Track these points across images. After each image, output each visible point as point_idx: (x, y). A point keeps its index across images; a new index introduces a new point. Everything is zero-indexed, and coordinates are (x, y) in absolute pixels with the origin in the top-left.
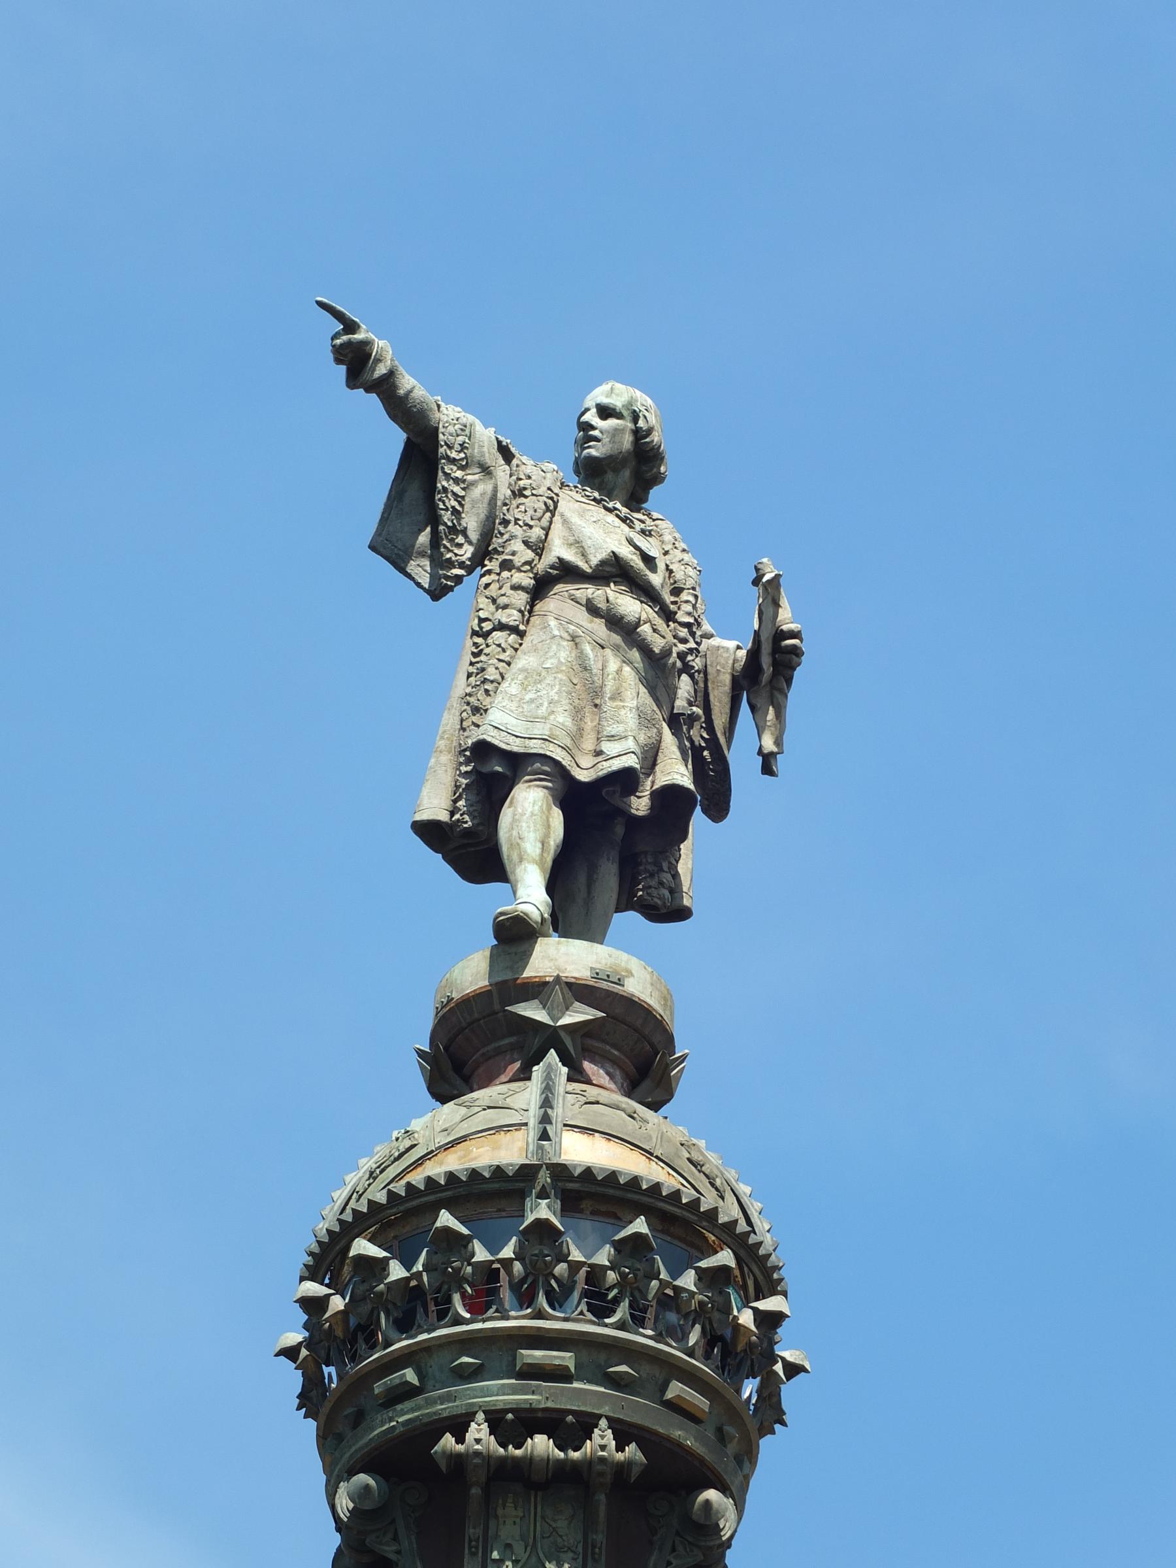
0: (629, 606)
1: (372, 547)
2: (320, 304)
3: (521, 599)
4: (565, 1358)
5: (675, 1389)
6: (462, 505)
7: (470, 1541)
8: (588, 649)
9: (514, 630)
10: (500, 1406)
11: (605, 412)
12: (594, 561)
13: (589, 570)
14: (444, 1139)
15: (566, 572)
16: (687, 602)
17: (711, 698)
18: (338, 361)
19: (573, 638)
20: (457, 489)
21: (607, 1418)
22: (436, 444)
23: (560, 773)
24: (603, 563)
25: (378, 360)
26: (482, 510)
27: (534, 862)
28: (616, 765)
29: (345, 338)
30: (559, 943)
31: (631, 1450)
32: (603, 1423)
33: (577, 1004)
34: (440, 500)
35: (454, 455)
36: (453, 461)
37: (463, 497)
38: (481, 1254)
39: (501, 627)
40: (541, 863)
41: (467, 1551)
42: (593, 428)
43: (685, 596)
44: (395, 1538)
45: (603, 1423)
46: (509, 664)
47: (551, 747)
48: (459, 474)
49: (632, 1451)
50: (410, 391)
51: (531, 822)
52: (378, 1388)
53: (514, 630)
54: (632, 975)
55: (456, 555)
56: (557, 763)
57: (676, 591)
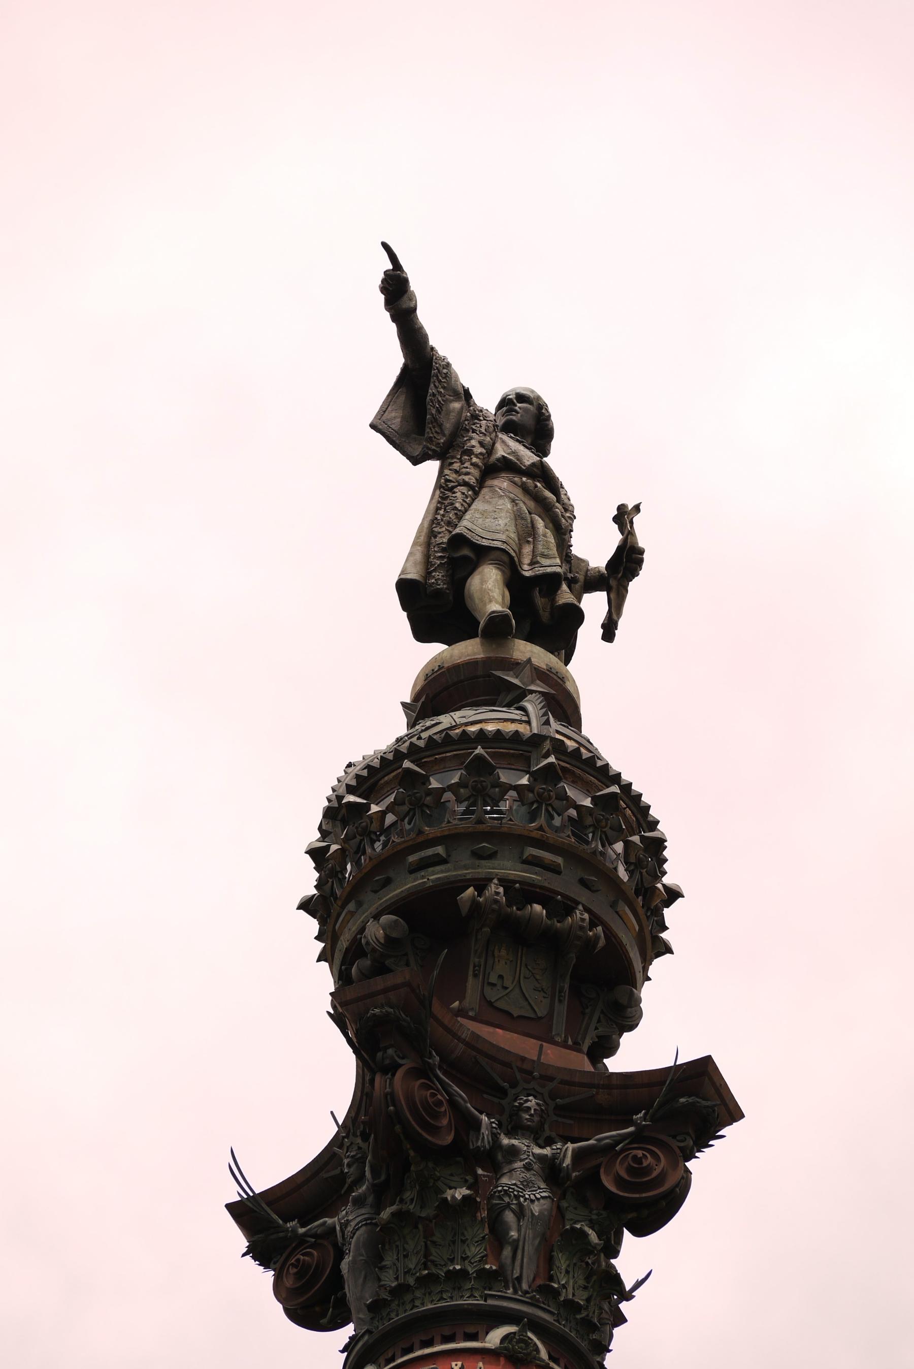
1: (372, 426)
3: (476, 472)
7: (475, 966)
10: (512, 877)
14: (464, 720)
15: (508, 466)
18: (383, 289)
19: (513, 501)
21: (583, 906)
28: (549, 570)
33: (538, 682)
36: (440, 381)
41: (471, 973)
44: (408, 964)
46: (470, 505)
51: (489, 590)
52: (412, 858)
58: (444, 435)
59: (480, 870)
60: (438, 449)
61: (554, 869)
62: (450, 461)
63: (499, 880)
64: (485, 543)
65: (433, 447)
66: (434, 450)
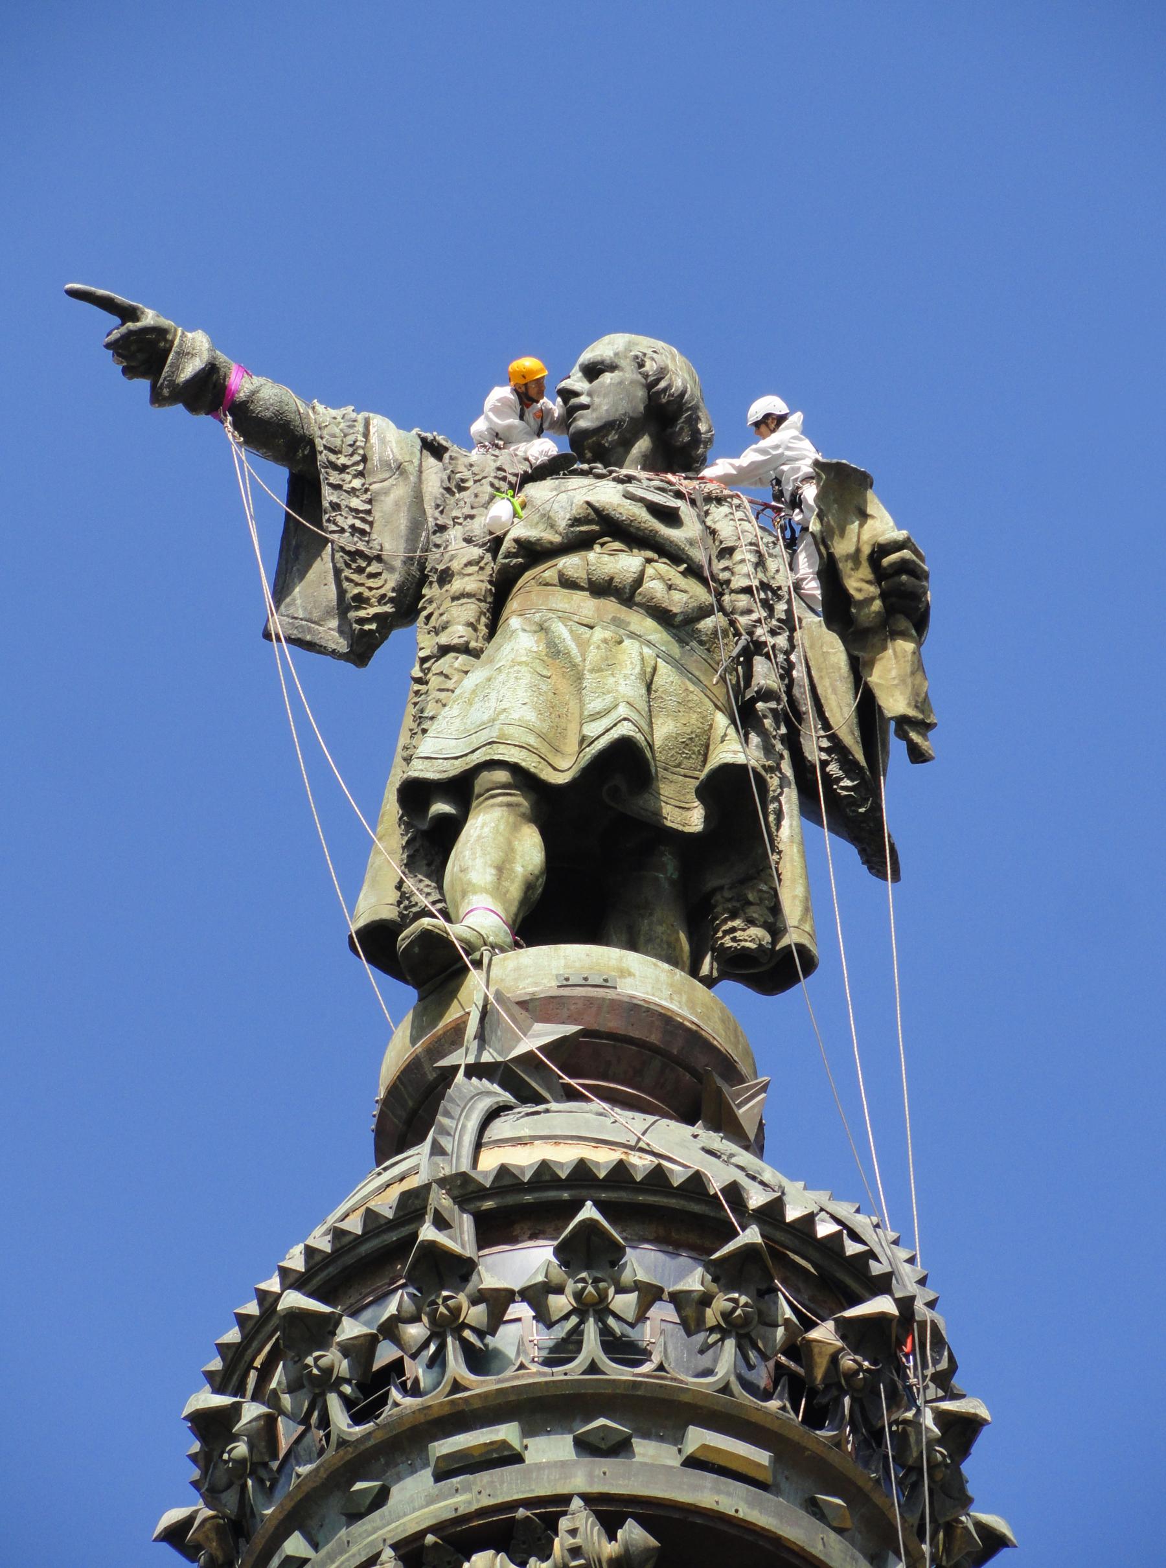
0: (623, 563)
2: (73, 294)
3: (469, 611)
4: (507, 1432)
5: (698, 1438)
6: (371, 524)
8: (561, 630)
9: (465, 649)
11: (592, 371)
12: (562, 524)
13: (557, 539)
16: (742, 561)
17: (820, 691)
18: (130, 372)
19: (542, 628)
20: (355, 503)
22: (314, 452)
23: (523, 779)
24: (576, 521)
25: (183, 354)
26: (403, 522)
27: (486, 891)
29: (123, 330)
30: (504, 959)
31: (633, 1533)
32: (577, 1503)
34: (329, 521)
35: (342, 460)
36: (343, 469)
37: (369, 512)
38: (350, 1329)
39: (444, 650)
40: (497, 890)
42: (576, 394)
43: (737, 556)
45: (577, 1503)
47: (502, 749)
48: (357, 483)
49: (633, 1533)
50: (253, 393)
53: (465, 649)
54: (630, 974)
55: (371, 589)
56: (515, 769)
57: (727, 552)
58: (391, 569)
59: (354, 1549)
60: (388, 608)
61: (508, 1457)
62: (425, 613)
63: (394, 1547)
64: (454, 769)
65: (372, 611)
66: (376, 617)
